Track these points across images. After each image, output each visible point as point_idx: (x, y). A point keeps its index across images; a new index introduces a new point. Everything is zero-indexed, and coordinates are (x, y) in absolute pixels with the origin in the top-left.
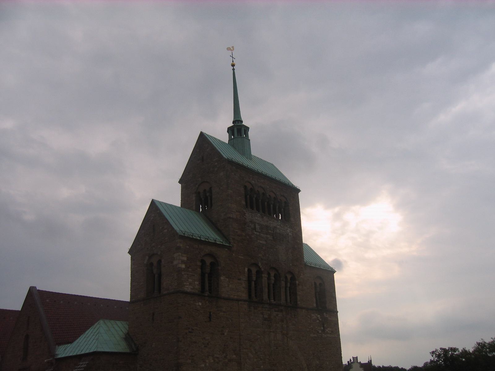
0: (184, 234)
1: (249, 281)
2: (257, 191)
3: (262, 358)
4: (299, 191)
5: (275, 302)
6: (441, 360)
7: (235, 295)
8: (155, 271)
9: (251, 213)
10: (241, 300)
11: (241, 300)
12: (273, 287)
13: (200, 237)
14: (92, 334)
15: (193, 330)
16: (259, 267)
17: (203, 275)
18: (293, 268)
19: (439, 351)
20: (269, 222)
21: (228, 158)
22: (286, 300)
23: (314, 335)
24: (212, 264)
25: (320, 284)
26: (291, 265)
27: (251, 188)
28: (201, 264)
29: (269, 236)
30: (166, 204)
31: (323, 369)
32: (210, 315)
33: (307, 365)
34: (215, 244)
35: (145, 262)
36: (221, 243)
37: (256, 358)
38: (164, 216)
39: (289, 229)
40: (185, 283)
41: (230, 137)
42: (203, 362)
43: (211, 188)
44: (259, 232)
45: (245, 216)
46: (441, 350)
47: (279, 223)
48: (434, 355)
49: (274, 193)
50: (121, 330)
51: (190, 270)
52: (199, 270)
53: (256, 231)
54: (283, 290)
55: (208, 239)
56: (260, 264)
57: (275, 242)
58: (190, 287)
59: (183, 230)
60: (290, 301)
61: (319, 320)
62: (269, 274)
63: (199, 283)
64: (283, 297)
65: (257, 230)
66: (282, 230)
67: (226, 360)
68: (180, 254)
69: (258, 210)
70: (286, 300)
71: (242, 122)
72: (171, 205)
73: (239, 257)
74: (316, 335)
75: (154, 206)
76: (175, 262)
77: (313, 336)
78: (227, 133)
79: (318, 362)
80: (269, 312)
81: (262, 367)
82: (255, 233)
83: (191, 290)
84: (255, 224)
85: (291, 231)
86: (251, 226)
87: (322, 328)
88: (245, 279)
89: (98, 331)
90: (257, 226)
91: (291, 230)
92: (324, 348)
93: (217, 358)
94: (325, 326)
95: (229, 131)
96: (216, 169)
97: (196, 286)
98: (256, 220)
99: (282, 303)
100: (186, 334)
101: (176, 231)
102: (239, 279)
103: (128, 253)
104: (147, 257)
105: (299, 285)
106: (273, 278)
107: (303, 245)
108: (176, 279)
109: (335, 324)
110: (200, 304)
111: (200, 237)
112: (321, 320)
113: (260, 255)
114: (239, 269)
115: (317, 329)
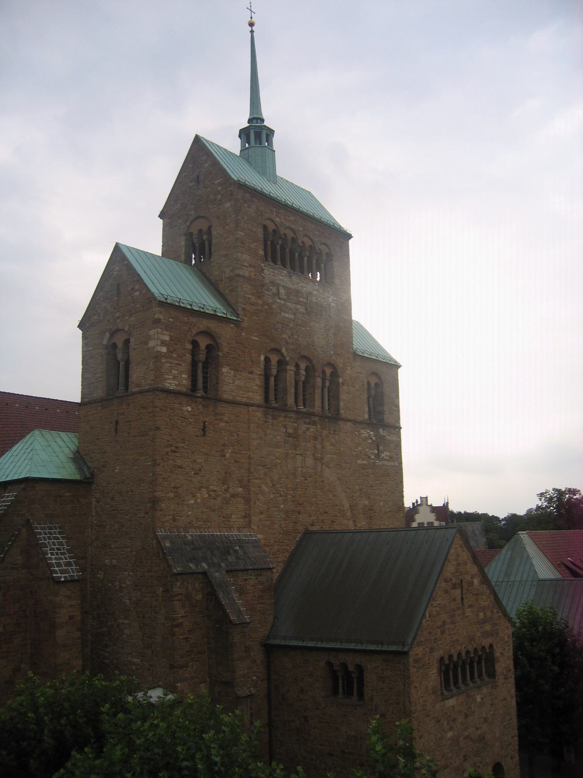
0: (166, 299)
1: (267, 376)
2: (285, 234)
3: (282, 492)
4: (350, 236)
5: (305, 410)
6: (553, 507)
7: (243, 397)
8: (120, 356)
9: (273, 269)
10: (252, 405)
11: (252, 405)
12: (303, 387)
13: (191, 305)
14: (22, 452)
15: (177, 447)
16: (282, 354)
17: (194, 364)
18: (335, 358)
19: (552, 493)
20: (301, 284)
21: (239, 180)
22: (322, 408)
23: (364, 462)
24: (209, 348)
25: (377, 385)
26: (332, 353)
27: (274, 231)
28: (192, 346)
29: (300, 307)
30: (137, 251)
31: (375, 512)
32: (204, 427)
33: (350, 506)
34: (214, 317)
35: (105, 342)
36: (224, 316)
37: (274, 493)
38: (134, 270)
39: (331, 296)
40: (166, 376)
41: (243, 145)
42: (193, 496)
43: (210, 227)
44: (284, 300)
45: (262, 274)
46: (553, 492)
47: (317, 287)
48: (543, 498)
50: (68, 446)
51: (174, 355)
52: (188, 357)
53: (279, 298)
54: (318, 392)
55: (203, 309)
56: (284, 351)
57: (308, 316)
58: (174, 382)
59: (164, 292)
60: (329, 409)
61: (371, 438)
62: (297, 366)
63: (188, 377)
64: (318, 403)
65: (280, 296)
66: (320, 298)
67: (228, 495)
68: (160, 330)
69: (284, 265)
70: (322, 408)
71: (263, 120)
72: (146, 253)
73: (252, 337)
74: (365, 462)
75: (119, 255)
76: (151, 344)
78: (239, 138)
79: (367, 502)
80: (296, 424)
81: (282, 506)
82: (278, 301)
83: (174, 387)
84: (278, 288)
86: (271, 290)
87: (376, 452)
88: (260, 373)
89: (32, 445)
90: (282, 291)
91: (335, 298)
92: (378, 482)
93: (214, 491)
94: (381, 448)
95: (242, 135)
96: (219, 197)
97: (184, 381)
98: (280, 280)
99: (316, 411)
100: (167, 453)
101: (153, 294)
102: (251, 373)
103: (78, 327)
104: (108, 335)
105: (343, 384)
106: (303, 372)
107: (353, 324)
108: (152, 370)
109: (396, 446)
110: (189, 409)
111: (191, 305)
113: (285, 336)
114: (251, 357)
115: (368, 453)
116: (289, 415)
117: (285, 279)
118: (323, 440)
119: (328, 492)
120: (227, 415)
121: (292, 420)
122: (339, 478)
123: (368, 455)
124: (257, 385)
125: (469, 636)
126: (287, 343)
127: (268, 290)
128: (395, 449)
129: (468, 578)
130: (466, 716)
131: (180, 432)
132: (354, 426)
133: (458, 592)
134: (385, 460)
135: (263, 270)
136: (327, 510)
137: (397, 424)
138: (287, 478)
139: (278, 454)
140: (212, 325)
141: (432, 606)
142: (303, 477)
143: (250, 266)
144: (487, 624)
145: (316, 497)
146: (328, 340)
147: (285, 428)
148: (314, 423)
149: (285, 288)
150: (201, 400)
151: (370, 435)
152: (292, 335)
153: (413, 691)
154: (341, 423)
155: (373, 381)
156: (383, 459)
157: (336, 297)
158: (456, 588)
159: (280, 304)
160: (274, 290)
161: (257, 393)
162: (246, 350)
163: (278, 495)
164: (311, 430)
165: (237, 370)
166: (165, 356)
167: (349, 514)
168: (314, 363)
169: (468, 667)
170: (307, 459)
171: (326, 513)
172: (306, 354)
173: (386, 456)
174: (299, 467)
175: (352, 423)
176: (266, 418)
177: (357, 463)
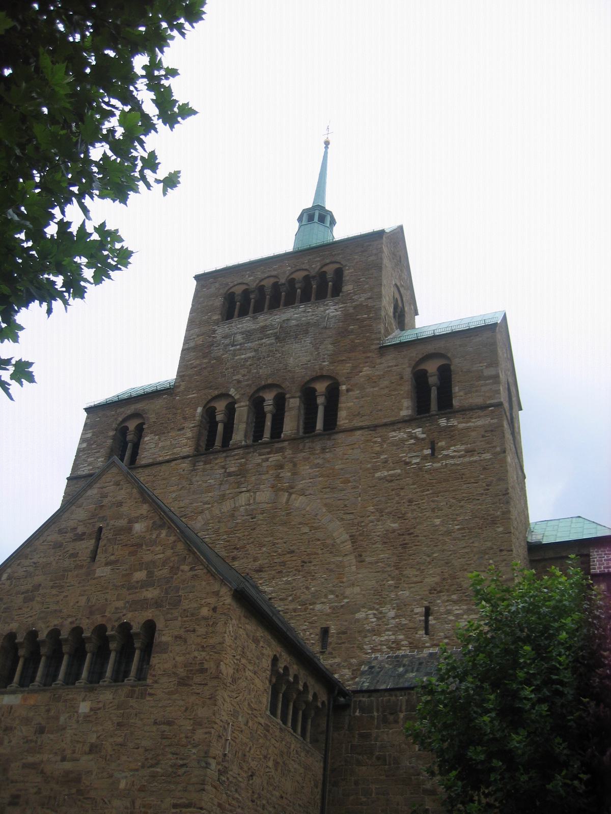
16: (230, 396)
23: (392, 472)
33: (350, 536)
49: (306, 270)
52: (109, 442)
53: (232, 346)
56: (232, 392)
61: (416, 438)
77: (386, 474)
79: (396, 525)
80: (243, 460)
82: (232, 348)
85: (341, 307)
87: (428, 452)
88: (193, 425)
91: (340, 306)
112: (424, 436)
114: (183, 415)
115: (404, 459)
116: (233, 453)
117: (245, 325)
118: (295, 465)
119: (300, 526)
121: (237, 457)
122: (326, 505)
123: (404, 461)
124: (188, 438)
126: (239, 382)
127: (219, 345)
128: (483, 436)
129: (122, 523)
130: (41, 730)
132: (374, 432)
134: (453, 457)
135: (214, 331)
136: (291, 548)
137: (488, 402)
138: (219, 522)
139: (208, 498)
140: (139, 406)
141: (19, 565)
142: (247, 516)
143: (198, 336)
144: (150, 589)
145: (272, 536)
146: (319, 353)
147: (223, 468)
148: (282, 450)
149: (242, 333)
151: (412, 436)
152: (249, 372)
154: (341, 437)
155: (432, 367)
156: (447, 457)
157: (344, 303)
158: (83, 540)
159: (234, 350)
160: (227, 341)
161: (186, 445)
162: (179, 411)
164: (270, 460)
165: (164, 433)
166: (84, 450)
167: (348, 546)
168: (283, 386)
169: (291, 707)
170: (258, 494)
171: (292, 552)
172: (270, 381)
173: (455, 451)
174: (241, 506)
175: (366, 430)
177: (374, 476)
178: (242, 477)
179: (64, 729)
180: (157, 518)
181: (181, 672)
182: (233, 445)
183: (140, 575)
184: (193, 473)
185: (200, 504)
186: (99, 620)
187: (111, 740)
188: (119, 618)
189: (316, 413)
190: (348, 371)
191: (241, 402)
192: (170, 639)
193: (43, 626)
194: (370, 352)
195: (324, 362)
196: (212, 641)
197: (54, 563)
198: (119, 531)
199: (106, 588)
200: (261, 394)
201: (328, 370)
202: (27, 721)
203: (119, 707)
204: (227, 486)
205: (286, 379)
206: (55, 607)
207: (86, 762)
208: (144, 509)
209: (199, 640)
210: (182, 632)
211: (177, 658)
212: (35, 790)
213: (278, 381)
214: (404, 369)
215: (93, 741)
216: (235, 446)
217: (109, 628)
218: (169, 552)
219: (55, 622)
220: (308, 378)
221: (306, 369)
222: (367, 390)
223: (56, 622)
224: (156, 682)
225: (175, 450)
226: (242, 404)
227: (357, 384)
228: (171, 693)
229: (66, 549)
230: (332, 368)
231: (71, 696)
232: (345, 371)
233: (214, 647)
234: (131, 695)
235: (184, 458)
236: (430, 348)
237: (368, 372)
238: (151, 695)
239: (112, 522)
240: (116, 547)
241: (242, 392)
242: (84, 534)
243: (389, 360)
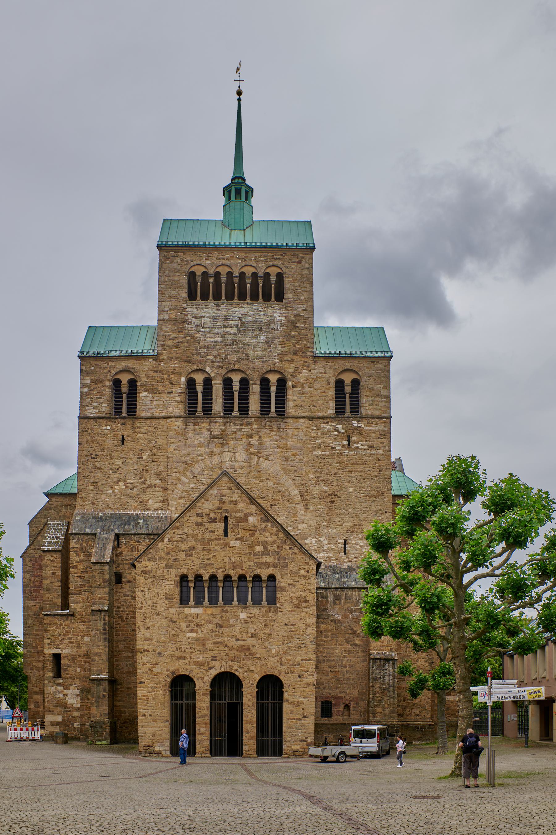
3: (204, 482)
16: (207, 373)
40: (87, 408)
52: (108, 392)
63: (108, 406)
80: (223, 427)
88: (180, 391)
110: (109, 428)
116: (215, 421)
120: (145, 428)
121: (218, 424)
125: (233, 563)
129: (240, 515)
130: (221, 626)
131: (99, 445)
133: (219, 527)
147: (209, 431)
150: (119, 420)
153: (138, 593)
158: (216, 522)
163: (200, 484)
165: (156, 393)
172: (237, 367)
176: (186, 425)
178: (224, 440)
179: (234, 626)
180: (263, 516)
181: (295, 601)
182: (215, 414)
183: (259, 548)
184: (186, 430)
185: (195, 455)
186: (241, 572)
187: (263, 632)
188: (253, 572)
189: (270, 396)
190: (293, 370)
191: (216, 380)
192: (286, 585)
193: (204, 572)
194: (307, 358)
195: (275, 359)
196: (309, 588)
197: (200, 535)
198: (239, 521)
199: (240, 554)
200: (229, 375)
201: (278, 367)
202: (210, 622)
203: (263, 616)
204: (214, 445)
205: (249, 368)
206: (209, 562)
207: (250, 642)
208: (253, 508)
209: (302, 586)
210: (292, 582)
211: (292, 595)
212: (225, 654)
213: (243, 368)
214: (330, 377)
215: (253, 631)
216: (216, 416)
217: (248, 577)
218: (275, 537)
219: (211, 571)
220: (265, 371)
221: (263, 362)
222: (306, 389)
223: (213, 571)
224: (282, 605)
225: (168, 410)
226: (218, 382)
227: (299, 382)
228: (291, 611)
229: (206, 527)
230: (281, 365)
231: (233, 610)
232: (290, 370)
233: (310, 590)
234: (269, 611)
235: (177, 417)
236: (348, 364)
237: (306, 374)
238: (280, 611)
239: (233, 514)
240: (240, 530)
241: (216, 371)
242: (215, 519)
243: (320, 366)
